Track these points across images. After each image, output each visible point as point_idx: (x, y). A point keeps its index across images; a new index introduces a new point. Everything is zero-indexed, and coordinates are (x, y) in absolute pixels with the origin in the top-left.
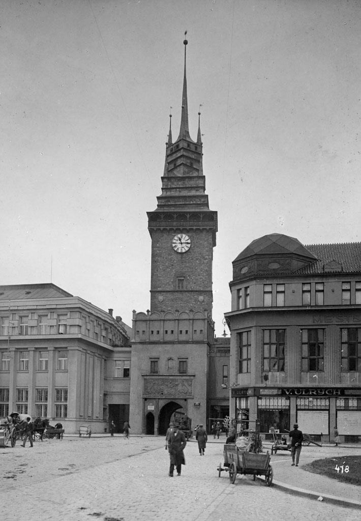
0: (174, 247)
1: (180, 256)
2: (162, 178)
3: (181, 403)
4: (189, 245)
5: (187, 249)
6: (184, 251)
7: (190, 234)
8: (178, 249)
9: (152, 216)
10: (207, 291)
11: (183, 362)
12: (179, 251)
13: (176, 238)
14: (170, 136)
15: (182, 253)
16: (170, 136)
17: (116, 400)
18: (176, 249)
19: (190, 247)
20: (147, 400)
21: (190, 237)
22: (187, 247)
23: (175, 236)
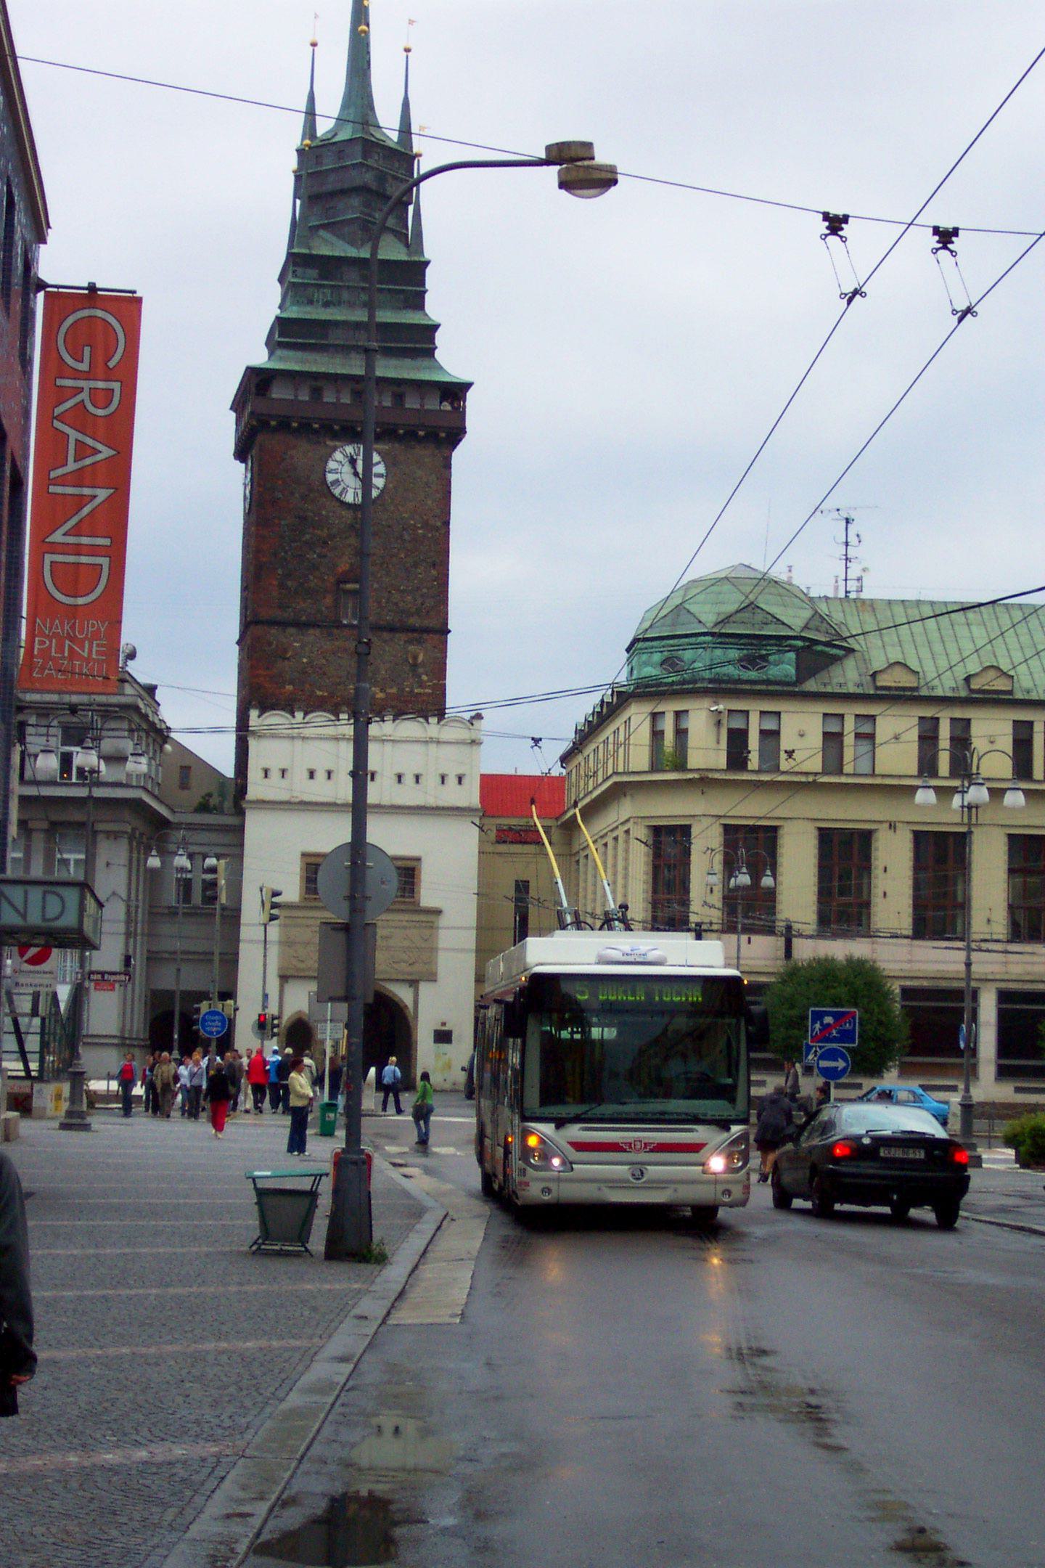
1: (347, 515)
3: (403, 994)
8: (344, 491)
10: (428, 631)
13: (338, 455)
14: (311, 114)
16: (311, 114)
18: (337, 492)
23: (335, 449)
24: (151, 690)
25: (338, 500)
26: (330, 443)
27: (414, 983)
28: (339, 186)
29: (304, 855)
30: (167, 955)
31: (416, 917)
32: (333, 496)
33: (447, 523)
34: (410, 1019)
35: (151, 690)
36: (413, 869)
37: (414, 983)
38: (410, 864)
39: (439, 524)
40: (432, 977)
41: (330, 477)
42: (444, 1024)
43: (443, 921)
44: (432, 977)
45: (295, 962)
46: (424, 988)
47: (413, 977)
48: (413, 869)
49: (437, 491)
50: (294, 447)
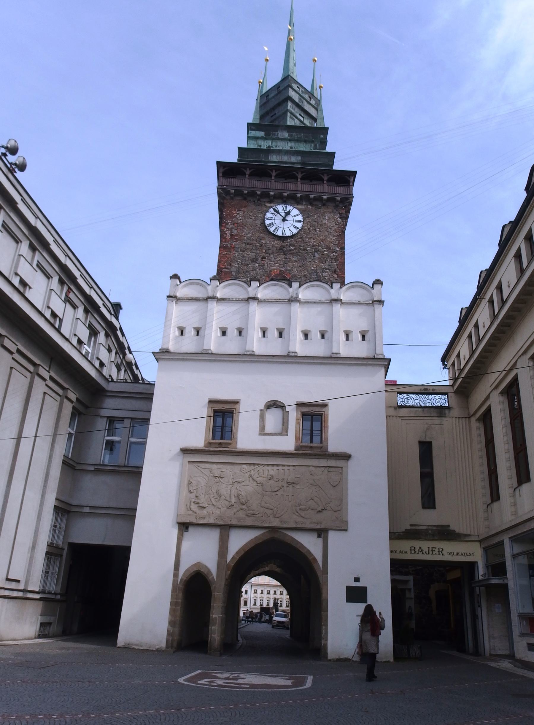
0: (269, 225)
1: (278, 244)
2: (249, 124)
3: (310, 543)
4: (299, 225)
5: (295, 231)
6: (288, 234)
7: (299, 207)
9: (225, 170)
11: (313, 415)
12: (279, 233)
15: (283, 238)
17: (91, 532)
18: (272, 230)
19: (302, 228)
20: (191, 529)
21: (302, 212)
22: (296, 227)
24: (117, 308)
25: (273, 234)
26: (268, 205)
27: (322, 533)
28: (278, 102)
29: (211, 402)
30: (87, 510)
31: (323, 462)
32: (270, 232)
33: (343, 249)
34: (319, 574)
35: (117, 308)
36: (321, 415)
37: (322, 533)
38: (317, 410)
39: (338, 249)
40: (343, 528)
41: (267, 222)
42: (357, 580)
43: (352, 466)
44: (342, 527)
45: (194, 507)
46: (332, 536)
47: (323, 526)
48: (321, 415)
49: (336, 231)
50: (245, 207)
